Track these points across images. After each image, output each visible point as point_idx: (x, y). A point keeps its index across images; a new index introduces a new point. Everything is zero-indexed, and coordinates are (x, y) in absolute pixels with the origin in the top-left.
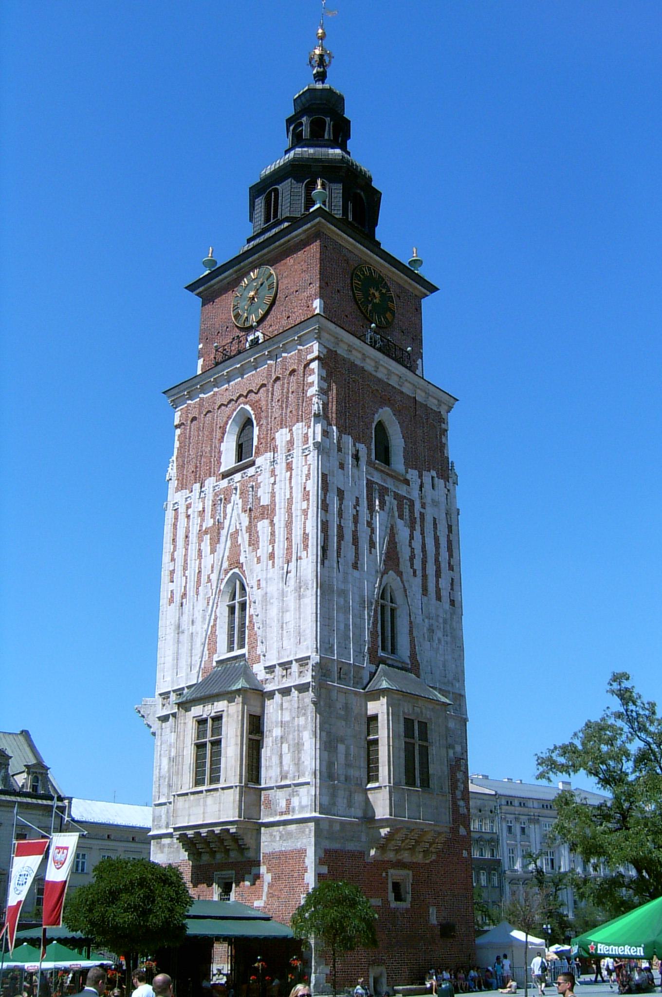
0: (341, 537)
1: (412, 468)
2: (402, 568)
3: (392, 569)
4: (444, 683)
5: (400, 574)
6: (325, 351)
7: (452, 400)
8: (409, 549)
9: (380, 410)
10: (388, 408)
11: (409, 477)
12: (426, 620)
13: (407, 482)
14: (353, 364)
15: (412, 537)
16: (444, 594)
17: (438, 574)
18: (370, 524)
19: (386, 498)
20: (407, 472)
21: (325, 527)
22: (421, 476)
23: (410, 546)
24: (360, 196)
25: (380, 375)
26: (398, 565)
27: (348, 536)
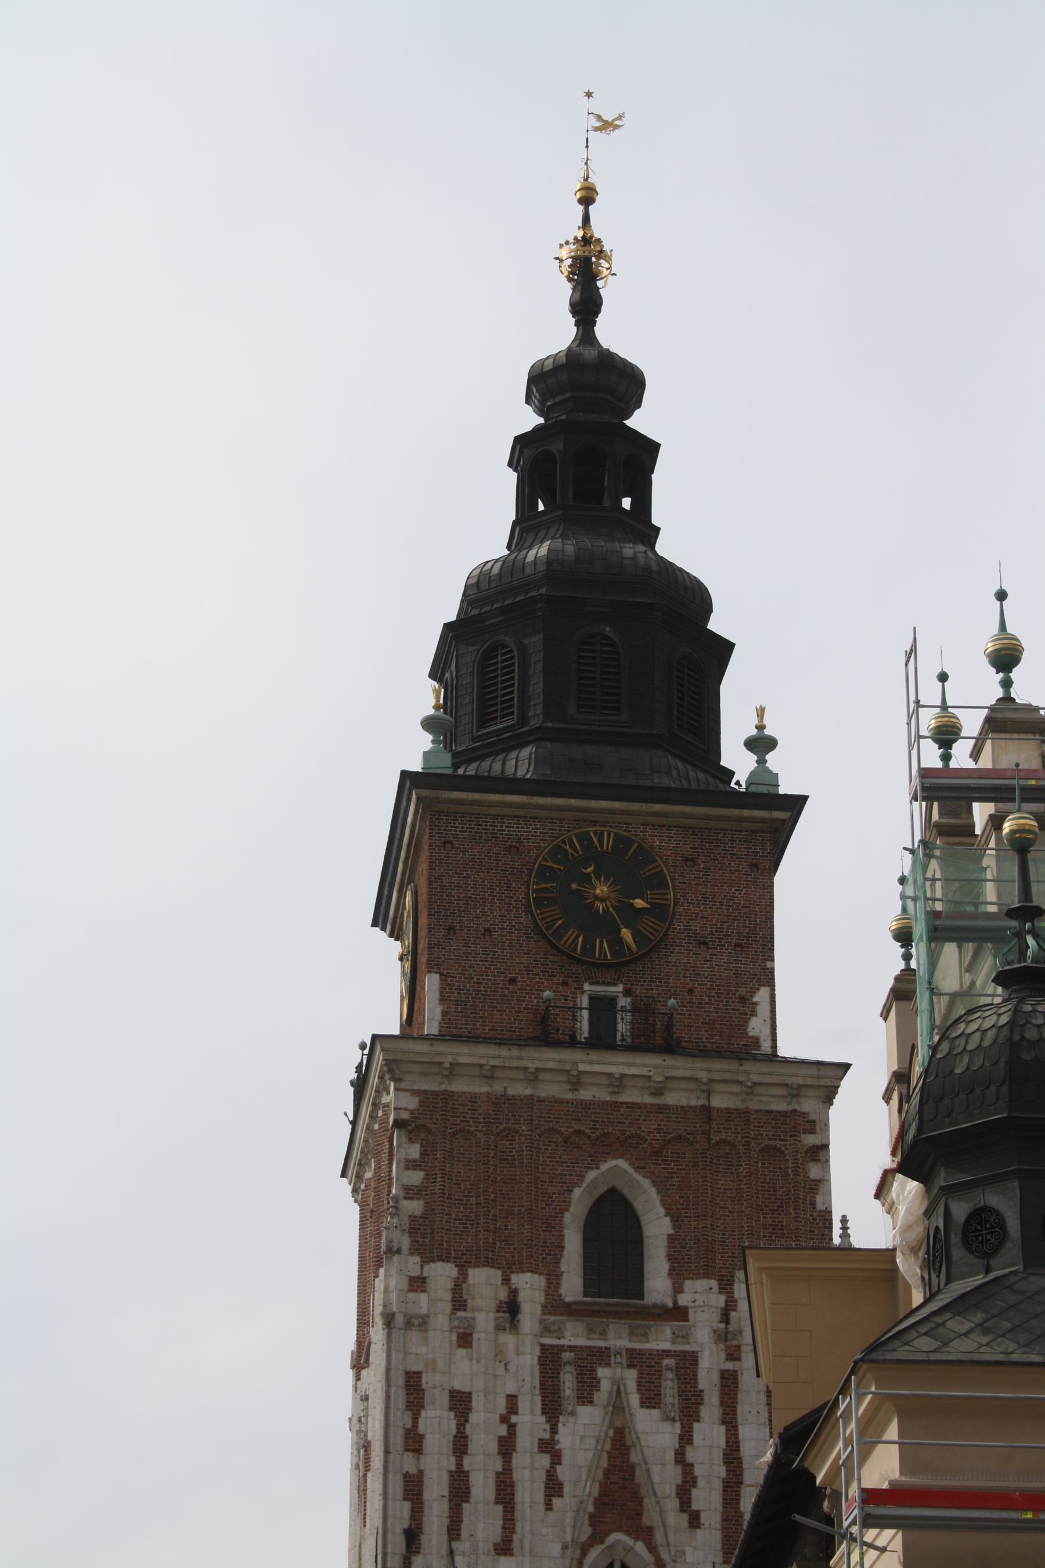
1: (698, 1276)
2: (650, 1517)
5: (645, 1534)
7: (830, 1072)
9: (591, 1175)
10: (622, 1163)
11: (683, 1300)
13: (679, 1313)
14: (500, 1102)
15: (686, 1438)
18: (548, 1446)
19: (602, 1372)
20: (678, 1289)
21: (413, 1488)
25: (586, 1094)
26: (639, 1514)
27: (482, 1486)
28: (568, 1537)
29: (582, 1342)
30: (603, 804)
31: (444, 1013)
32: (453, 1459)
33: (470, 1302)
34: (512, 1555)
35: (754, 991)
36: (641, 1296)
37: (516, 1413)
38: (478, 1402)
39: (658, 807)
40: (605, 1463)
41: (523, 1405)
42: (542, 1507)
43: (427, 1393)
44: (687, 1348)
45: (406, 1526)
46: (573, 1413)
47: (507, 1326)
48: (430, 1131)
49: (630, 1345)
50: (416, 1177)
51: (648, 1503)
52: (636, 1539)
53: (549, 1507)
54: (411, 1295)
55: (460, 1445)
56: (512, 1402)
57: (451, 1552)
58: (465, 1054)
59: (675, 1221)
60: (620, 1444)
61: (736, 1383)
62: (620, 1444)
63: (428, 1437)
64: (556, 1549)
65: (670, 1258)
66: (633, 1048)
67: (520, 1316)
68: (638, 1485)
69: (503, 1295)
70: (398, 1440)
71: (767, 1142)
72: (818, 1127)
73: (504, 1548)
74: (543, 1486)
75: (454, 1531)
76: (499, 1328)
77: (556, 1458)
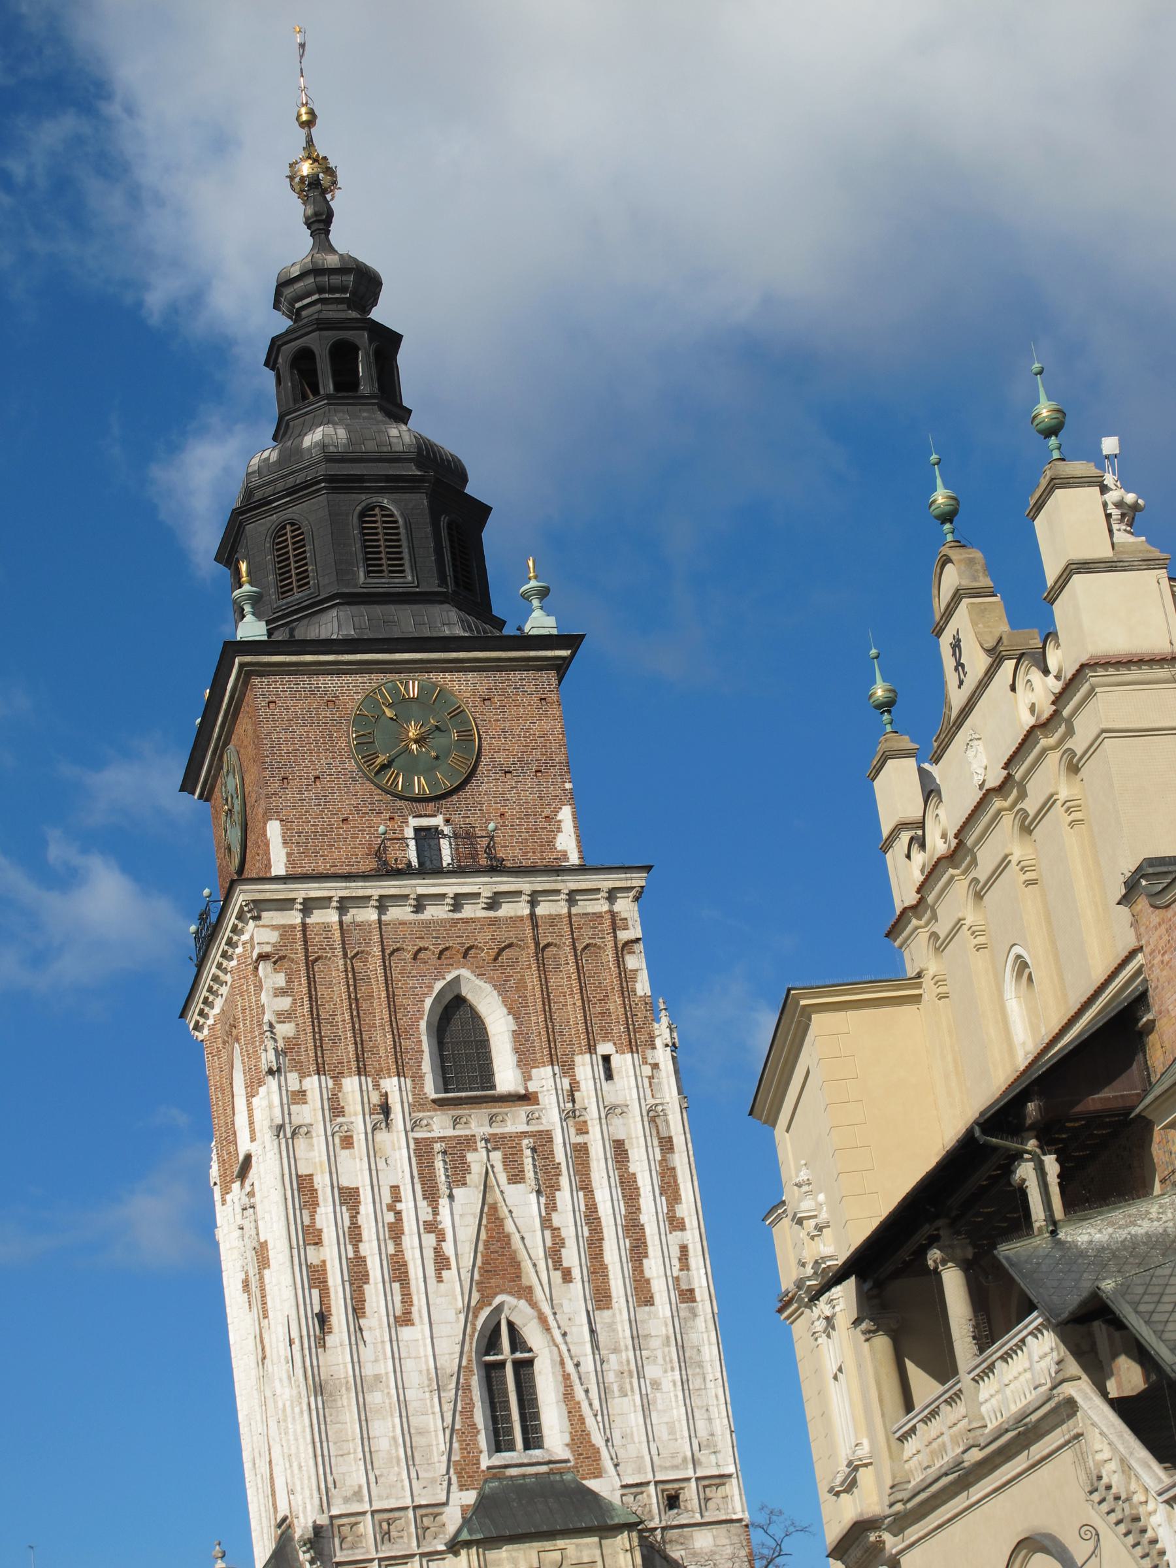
0: (357, 1275)
3: (502, 1292)
4: (675, 1467)
5: (527, 1293)
6: (274, 936)
8: (548, 1233)
10: (465, 972)
12: (613, 1358)
15: (551, 1206)
16: (659, 1287)
17: (638, 1252)
18: (432, 1227)
19: (470, 1157)
20: (527, 1078)
21: (316, 1277)
22: (568, 1069)
23: (546, 1223)
24: (383, 508)
26: (519, 1277)
28: (460, 1305)
29: (450, 1132)
31: (289, 855)
32: (350, 1248)
33: (346, 1109)
34: (413, 1325)
35: (557, 811)
36: (493, 1087)
37: (400, 1201)
38: (366, 1196)
39: (454, 655)
40: (483, 1236)
41: (406, 1192)
42: (432, 1280)
43: (320, 1193)
44: (541, 1128)
45: (317, 1310)
46: (451, 1197)
47: (383, 1125)
48: (292, 960)
49: (492, 1131)
50: (285, 1003)
51: (527, 1266)
52: (519, 1298)
53: (440, 1279)
54: (293, 1107)
57: (361, 1329)
58: (316, 890)
59: (517, 1018)
60: (492, 1217)
61: (587, 1153)
62: (492, 1217)
63: (325, 1230)
64: (451, 1315)
65: (517, 1051)
66: (459, 871)
67: (392, 1116)
68: (515, 1252)
69: (375, 1099)
70: (297, 1236)
71: (588, 941)
72: (630, 923)
73: (405, 1319)
74: (432, 1261)
75: (358, 1309)
76: (374, 1129)
77: (441, 1237)
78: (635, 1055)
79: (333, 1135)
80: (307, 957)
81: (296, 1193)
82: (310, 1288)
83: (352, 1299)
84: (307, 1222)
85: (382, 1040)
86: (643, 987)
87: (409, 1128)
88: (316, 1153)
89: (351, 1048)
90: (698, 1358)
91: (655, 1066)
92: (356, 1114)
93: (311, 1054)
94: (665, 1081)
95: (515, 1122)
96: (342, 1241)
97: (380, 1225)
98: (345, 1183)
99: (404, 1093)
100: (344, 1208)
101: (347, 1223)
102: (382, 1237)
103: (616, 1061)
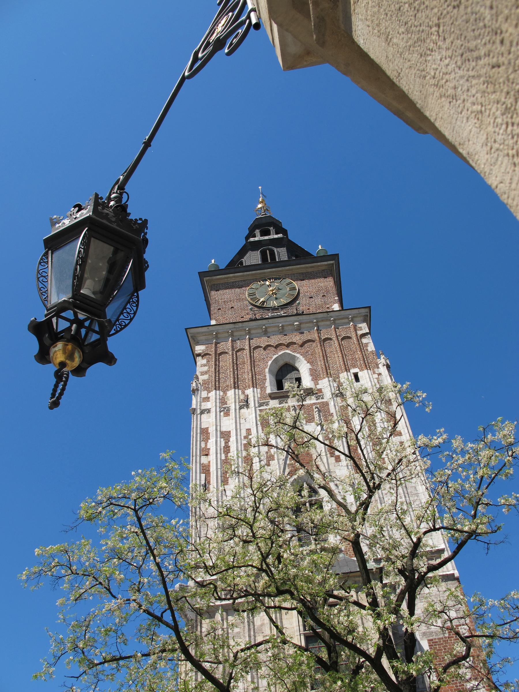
1: (324, 378)
10: (288, 351)
11: (319, 387)
20: (316, 384)
22: (336, 378)
30: (269, 270)
33: (228, 402)
41: (254, 431)
43: (211, 434)
44: (323, 400)
45: (203, 482)
48: (210, 355)
50: (206, 369)
55: (227, 449)
56: (249, 431)
65: (311, 375)
69: (242, 397)
72: (363, 328)
78: (369, 371)
79: (220, 412)
80: (216, 351)
81: (199, 435)
82: (200, 473)
83: (221, 477)
84: (203, 445)
85: (247, 377)
86: (371, 347)
87: (257, 405)
88: (211, 419)
89: (232, 380)
90: (416, 492)
91: (380, 374)
92: (232, 403)
93: (213, 383)
94: (385, 378)
95: (310, 401)
96: (219, 452)
97: (239, 444)
98: (224, 429)
99: (256, 394)
100: (222, 440)
101: (223, 444)
102: (239, 449)
103: (360, 375)
